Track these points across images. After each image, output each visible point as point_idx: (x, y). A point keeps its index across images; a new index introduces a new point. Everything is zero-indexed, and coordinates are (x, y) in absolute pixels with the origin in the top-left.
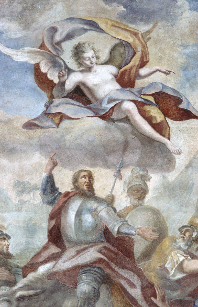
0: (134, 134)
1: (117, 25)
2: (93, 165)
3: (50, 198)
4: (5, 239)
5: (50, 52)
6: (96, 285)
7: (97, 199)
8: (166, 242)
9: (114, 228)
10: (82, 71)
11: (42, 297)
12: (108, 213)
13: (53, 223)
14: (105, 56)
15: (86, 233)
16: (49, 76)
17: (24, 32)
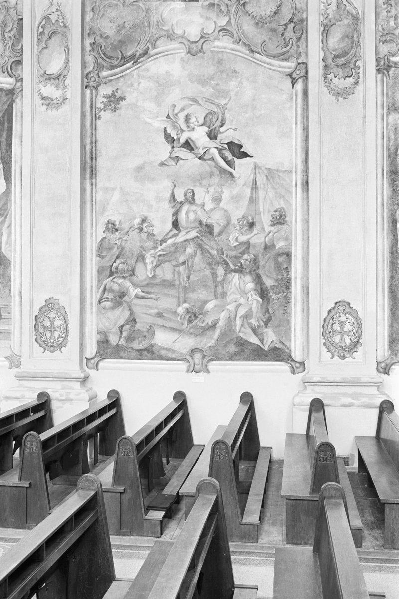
0: (216, 167)
1: (209, 101)
2: (194, 186)
3: (173, 204)
4: (151, 226)
5: (171, 119)
6: (195, 249)
7: (197, 205)
8: (231, 226)
9: (205, 220)
10: (189, 131)
11: (170, 254)
12: (202, 212)
13: (174, 218)
14: (201, 121)
15: (191, 223)
16: (172, 135)
17: (158, 108)
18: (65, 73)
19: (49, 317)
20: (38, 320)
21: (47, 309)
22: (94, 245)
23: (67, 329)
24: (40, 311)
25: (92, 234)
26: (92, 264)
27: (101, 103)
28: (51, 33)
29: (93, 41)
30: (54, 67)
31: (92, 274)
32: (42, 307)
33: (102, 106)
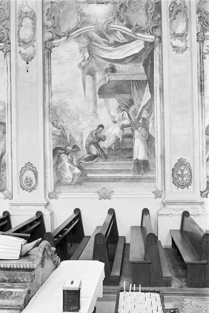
18: (186, 33)
19: (180, 169)
20: (174, 171)
21: (179, 164)
22: (204, 128)
23: (191, 175)
24: (175, 166)
25: (202, 122)
26: (203, 139)
27: (206, 50)
28: (177, 11)
29: (200, 15)
30: (180, 29)
31: (203, 144)
32: (176, 164)
33: (206, 52)
